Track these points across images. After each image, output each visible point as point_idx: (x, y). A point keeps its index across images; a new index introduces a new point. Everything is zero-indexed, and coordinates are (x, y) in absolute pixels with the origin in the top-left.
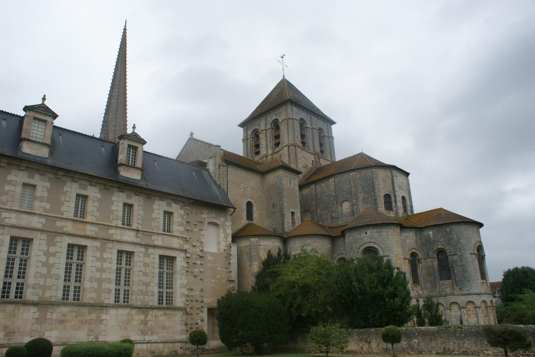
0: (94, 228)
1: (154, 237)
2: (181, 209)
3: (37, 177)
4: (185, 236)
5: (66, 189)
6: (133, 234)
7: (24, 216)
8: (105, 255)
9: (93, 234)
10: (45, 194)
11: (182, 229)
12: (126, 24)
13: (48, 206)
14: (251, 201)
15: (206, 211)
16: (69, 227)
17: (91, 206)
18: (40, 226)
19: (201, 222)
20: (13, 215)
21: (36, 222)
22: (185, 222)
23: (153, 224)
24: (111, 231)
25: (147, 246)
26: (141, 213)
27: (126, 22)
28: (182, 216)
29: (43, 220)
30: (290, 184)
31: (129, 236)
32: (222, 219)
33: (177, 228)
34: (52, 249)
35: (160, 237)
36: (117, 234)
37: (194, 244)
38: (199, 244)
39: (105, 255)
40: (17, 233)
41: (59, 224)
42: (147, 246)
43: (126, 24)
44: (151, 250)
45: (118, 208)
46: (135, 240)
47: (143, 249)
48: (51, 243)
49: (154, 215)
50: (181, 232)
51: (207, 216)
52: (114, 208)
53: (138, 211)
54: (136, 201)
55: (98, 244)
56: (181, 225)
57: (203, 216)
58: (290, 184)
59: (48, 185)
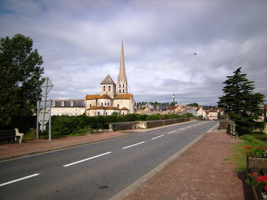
31: (72, 112)
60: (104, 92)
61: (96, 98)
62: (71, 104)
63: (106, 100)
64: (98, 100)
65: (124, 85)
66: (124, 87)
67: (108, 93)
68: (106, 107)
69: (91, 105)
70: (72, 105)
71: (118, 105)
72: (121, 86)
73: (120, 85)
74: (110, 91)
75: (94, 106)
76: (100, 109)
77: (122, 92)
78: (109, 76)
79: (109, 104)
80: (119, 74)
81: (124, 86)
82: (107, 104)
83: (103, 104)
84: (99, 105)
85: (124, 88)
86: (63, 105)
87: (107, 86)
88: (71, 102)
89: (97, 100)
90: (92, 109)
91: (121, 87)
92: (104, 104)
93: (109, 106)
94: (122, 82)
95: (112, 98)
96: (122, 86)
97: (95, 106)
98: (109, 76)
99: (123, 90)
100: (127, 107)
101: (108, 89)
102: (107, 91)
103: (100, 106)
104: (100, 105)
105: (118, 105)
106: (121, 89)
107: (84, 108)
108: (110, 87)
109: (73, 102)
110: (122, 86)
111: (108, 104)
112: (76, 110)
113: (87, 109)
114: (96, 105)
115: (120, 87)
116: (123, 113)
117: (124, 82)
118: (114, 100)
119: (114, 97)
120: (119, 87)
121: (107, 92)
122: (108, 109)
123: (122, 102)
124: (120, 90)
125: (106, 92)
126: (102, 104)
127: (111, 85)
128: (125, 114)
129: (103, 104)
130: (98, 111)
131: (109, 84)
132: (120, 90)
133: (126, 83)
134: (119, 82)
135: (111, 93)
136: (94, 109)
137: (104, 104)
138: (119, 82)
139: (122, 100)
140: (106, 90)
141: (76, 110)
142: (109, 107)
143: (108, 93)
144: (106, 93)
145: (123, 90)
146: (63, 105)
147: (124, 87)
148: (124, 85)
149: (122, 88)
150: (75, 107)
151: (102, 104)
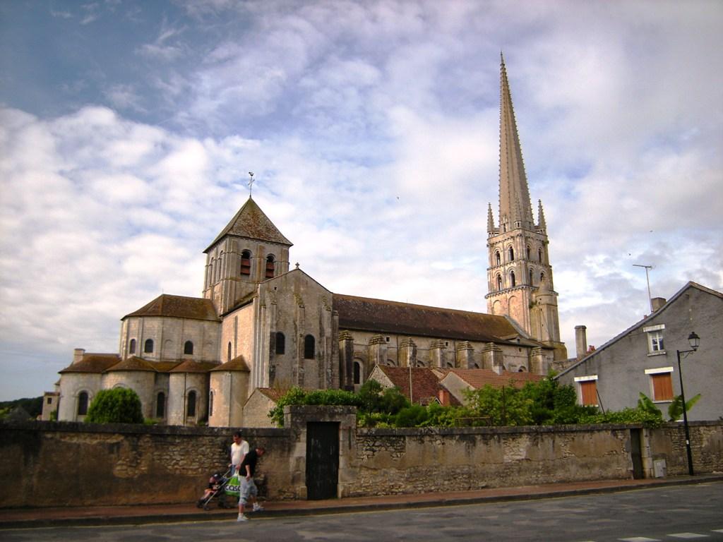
65: (512, 251)
66: (513, 259)
73: (498, 255)
77: (508, 284)
81: (515, 251)
85: (515, 265)
94: (500, 238)
96: (505, 256)
98: (251, 204)
99: (513, 276)
100: (248, 356)
132: (499, 278)
133: (518, 240)
134: (494, 240)
145: (513, 276)
147: (513, 259)
149: (507, 268)
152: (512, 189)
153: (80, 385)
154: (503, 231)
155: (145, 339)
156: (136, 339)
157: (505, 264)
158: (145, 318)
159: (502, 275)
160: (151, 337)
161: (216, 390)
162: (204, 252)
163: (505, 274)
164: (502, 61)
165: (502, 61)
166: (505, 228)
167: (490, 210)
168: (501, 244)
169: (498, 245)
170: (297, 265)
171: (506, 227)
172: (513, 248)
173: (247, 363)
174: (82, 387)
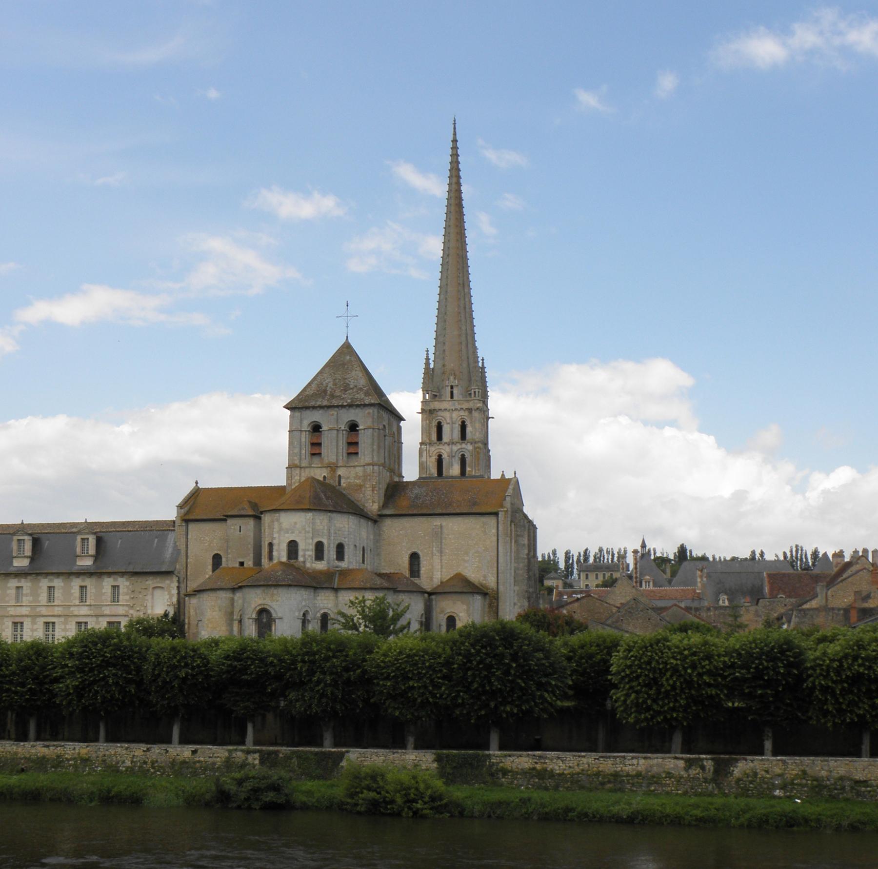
0: (60, 609)
1: (104, 608)
2: (127, 581)
3: (23, 580)
4: (129, 603)
5: (41, 584)
6: (86, 608)
7: (18, 608)
8: (68, 627)
9: (60, 613)
10: (29, 591)
11: (127, 597)
12: (455, 128)
13: (31, 598)
14: (219, 552)
15: (151, 578)
16: (44, 611)
17: (58, 594)
18: (27, 613)
19: (146, 589)
20: (13, 609)
21: (25, 611)
22: (130, 592)
23: (103, 598)
24: (72, 609)
25: (97, 616)
26: (94, 591)
27: (455, 124)
28: (127, 587)
29: (29, 609)
30: (240, 531)
31: (84, 611)
32: (168, 582)
33: (123, 598)
34: (35, 627)
35: (108, 608)
36: (75, 611)
37: (138, 609)
38: (142, 608)
39: (68, 627)
40: (17, 620)
41: (38, 609)
42: (97, 616)
43: (455, 128)
44: (100, 619)
45: (76, 591)
46: (88, 613)
47: (94, 619)
48: (34, 623)
49: (104, 591)
50: (127, 601)
51: (151, 582)
52: (73, 591)
53: (91, 590)
54: (88, 582)
55: (62, 619)
56: (127, 594)
57: (147, 583)
58: (240, 531)
59: (29, 584)
60: (316, 460)
61: (254, 506)
62: (78, 550)
63: (321, 521)
64: (267, 519)
65: (463, 427)
67: (341, 472)
68: (321, 572)
69: (217, 560)
70: (88, 562)
71: (414, 558)
72: (446, 429)
74: (354, 461)
75: (242, 564)
76: (277, 586)
77: (456, 470)
78: (347, 349)
79: (348, 552)
80: (432, 351)
81: (469, 429)
82: (330, 553)
83: (300, 553)
84: (271, 558)
85: (470, 447)
86: (21, 563)
87: (326, 420)
88: (79, 538)
89: (257, 518)
90: (219, 584)
91: (446, 438)
92: (306, 551)
93: (344, 565)
95: (373, 506)
96: (450, 432)
97: (249, 563)
98: (347, 349)
101: (342, 444)
102: (335, 461)
103: (275, 561)
104: (281, 554)
105: (414, 558)
106: (445, 451)
107: (172, 585)
108: (353, 427)
109: (92, 541)
110: (450, 432)
111: (340, 549)
112: (115, 598)
113: (192, 585)
114: (258, 562)
115: (440, 437)
116: (451, 621)
117: (470, 405)
118: (388, 522)
119: (385, 506)
120: (434, 437)
121: (333, 467)
122: (336, 590)
123: (438, 535)
124: (440, 461)
125: (326, 461)
126: (293, 547)
127: (364, 419)
128: (459, 625)
129: (301, 546)
130: (255, 599)
131: (350, 406)
132: (440, 461)
134: (436, 405)
135: (359, 470)
136: (234, 590)
137: (306, 551)
138: (436, 405)
139: (437, 522)
140: (324, 450)
141: (115, 598)
142: (344, 573)
143: (341, 472)
144: (325, 472)
146: (21, 563)
148: (463, 427)
149: (455, 448)
150: (110, 574)
151: (293, 547)
152: (463, 338)
153: (304, 604)
154: (449, 395)
155: (337, 542)
156: (325, 541)
157: (451, 443)
158: (334, 515)
159: (445, 456)
160: (345, 541)
161: (461, 615)
162: (286, 407)
163: (452, 456)
164: (455, 134)
165: (455, 134)
166: (452, 393)
167: (427, 359)
168: (447, 415)
169: (440, 413)
170: (515, 473)
171: (455, 391)
172: (468, 423)
173: (476, 584)
174: (305, 606)
